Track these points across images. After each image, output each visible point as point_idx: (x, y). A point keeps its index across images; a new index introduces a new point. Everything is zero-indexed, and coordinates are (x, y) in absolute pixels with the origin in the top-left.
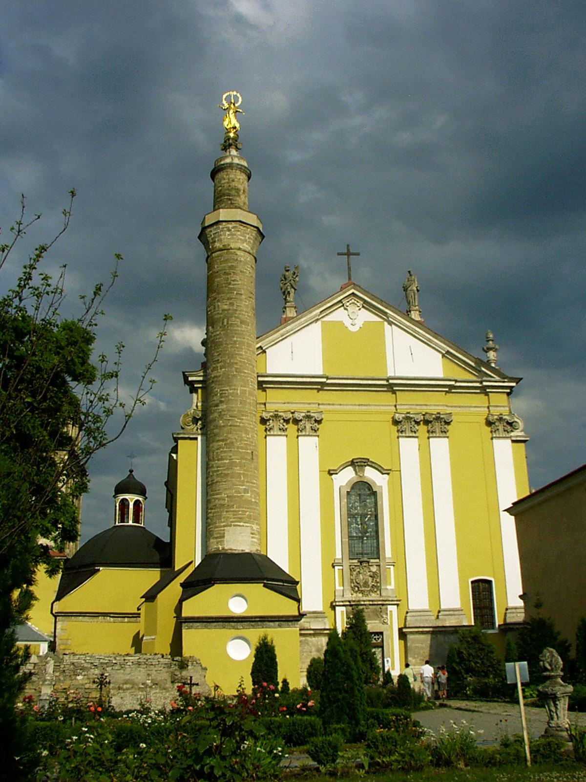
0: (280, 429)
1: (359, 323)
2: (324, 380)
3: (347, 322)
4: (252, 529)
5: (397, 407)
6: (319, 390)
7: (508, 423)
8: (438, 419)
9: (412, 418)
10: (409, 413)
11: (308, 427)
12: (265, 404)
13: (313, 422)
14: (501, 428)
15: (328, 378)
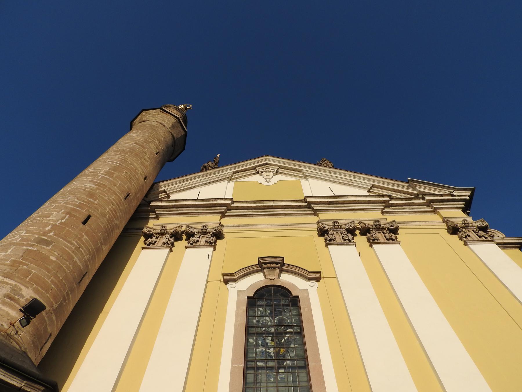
0: (164, 244)
8: (378, 226)
10: (337, 222)
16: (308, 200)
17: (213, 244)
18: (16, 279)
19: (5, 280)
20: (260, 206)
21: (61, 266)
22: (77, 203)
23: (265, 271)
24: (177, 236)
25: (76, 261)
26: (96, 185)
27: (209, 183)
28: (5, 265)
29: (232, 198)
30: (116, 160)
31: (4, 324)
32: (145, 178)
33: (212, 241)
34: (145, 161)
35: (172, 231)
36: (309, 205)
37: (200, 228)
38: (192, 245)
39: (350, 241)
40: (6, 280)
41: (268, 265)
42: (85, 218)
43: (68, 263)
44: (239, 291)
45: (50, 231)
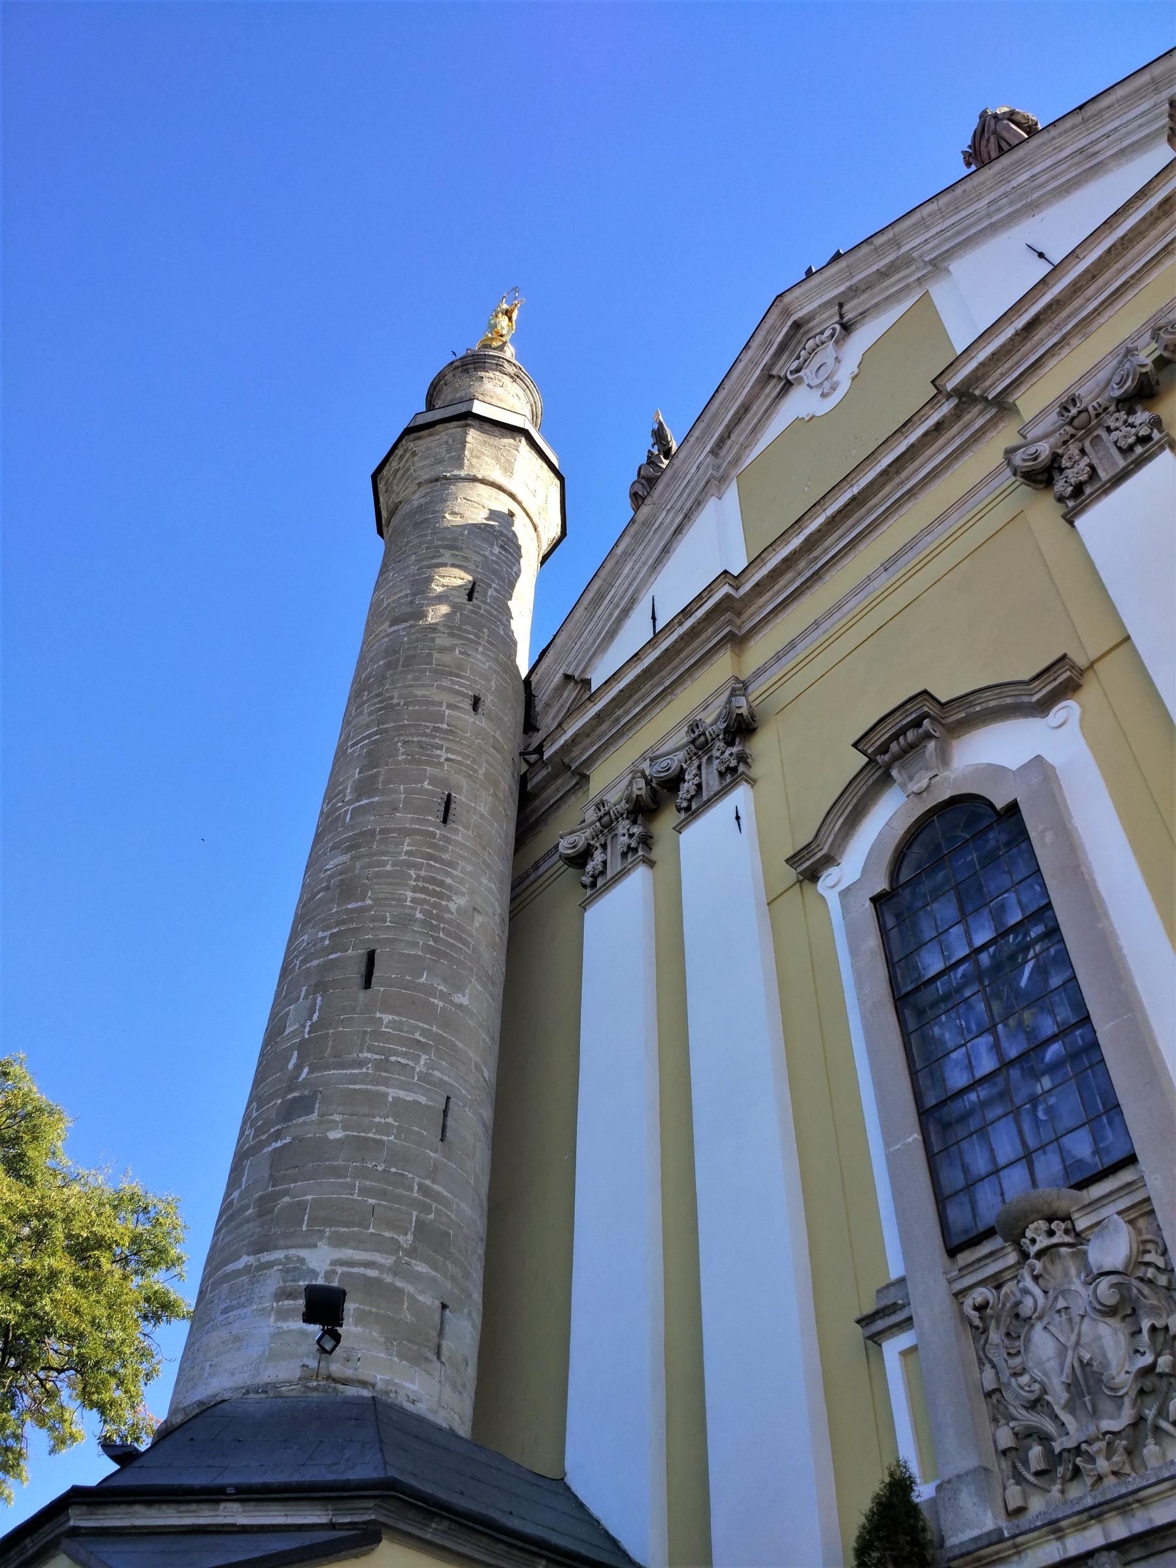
0: (624, 855)
10: (1073, 400)
16: (950, 386)
17: (741, 768)
18: (281, 1242)
19: (263, 1260)
20: (819, 530)
21: (366, 1139)
22: (327, 942)
23: (894, 773)
24: (644, 809)
25: (397, 1099)
26: (348, 850)
27: (666, 550)
28: (247, 1221)
29: (726, 572)
30: (368, 726)
31: (306, 1361)
32: (476, 703)
33: (733, 763)
34: (446, 658)
35: (624, 805)
36: (965, 396)
37: (686, 740)
38: (691, 813)
39: (1144, 440)
40: (266, 1257)
41: (894, 747)
42: (363, 968)
43: (377, 1119)
45: (299, 1067)
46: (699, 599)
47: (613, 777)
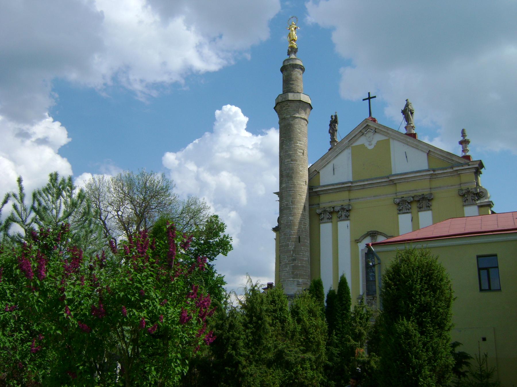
1: (374, 142)
2: (350, 185)
3: (367, 144)
4: (298, 282)
5: (397, 194)
6: (349, 191)
7: (474, 194)
9: (406, 201)
10: (403, 197)
11: (343, 216)
12: (319, 204)
13: (345, 211)
14: (469, 198)
15: (351, 182)
27: (337, 155)
36: (391, 180)
44: (362, 250)
46: (346, 183)
47: (326, 201)
